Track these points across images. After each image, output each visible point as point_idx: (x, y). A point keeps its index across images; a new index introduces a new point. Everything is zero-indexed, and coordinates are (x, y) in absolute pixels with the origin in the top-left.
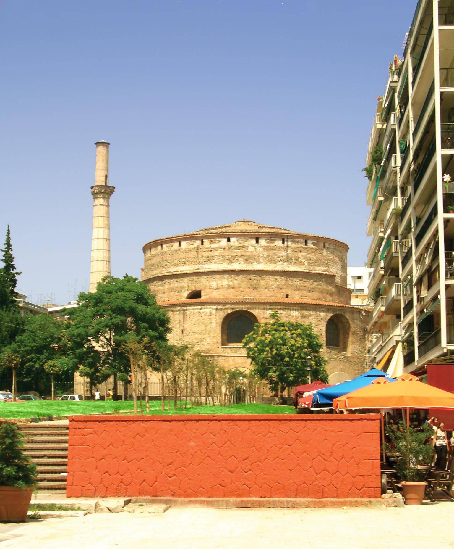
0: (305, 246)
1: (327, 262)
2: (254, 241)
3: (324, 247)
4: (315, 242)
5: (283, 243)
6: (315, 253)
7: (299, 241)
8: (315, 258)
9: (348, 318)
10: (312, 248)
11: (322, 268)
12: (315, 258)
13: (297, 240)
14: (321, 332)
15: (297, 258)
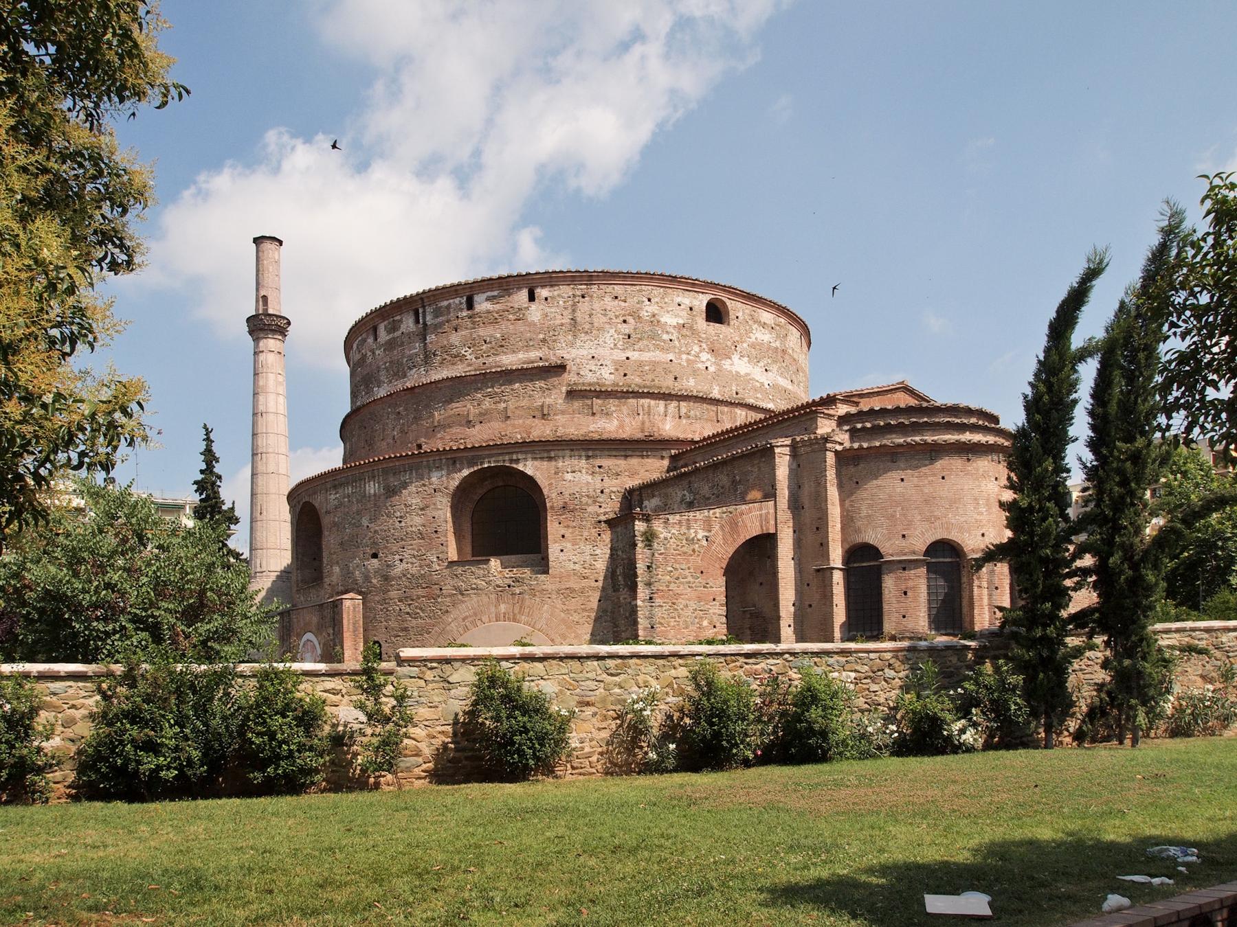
0: (465, 313)
1: (541, 336)
2: (370, 340)
3: (532, 298)
4: (495, 293)
5: (417, 321)
6: (495, 321)
7: (450, 304)
8: (498, 335)
9: (529, 472)
10: (488, 312)
11: (521, 356)
12: (498, 335)
13: (445, 303)
14: (435, 525)
15: (446, 349)
